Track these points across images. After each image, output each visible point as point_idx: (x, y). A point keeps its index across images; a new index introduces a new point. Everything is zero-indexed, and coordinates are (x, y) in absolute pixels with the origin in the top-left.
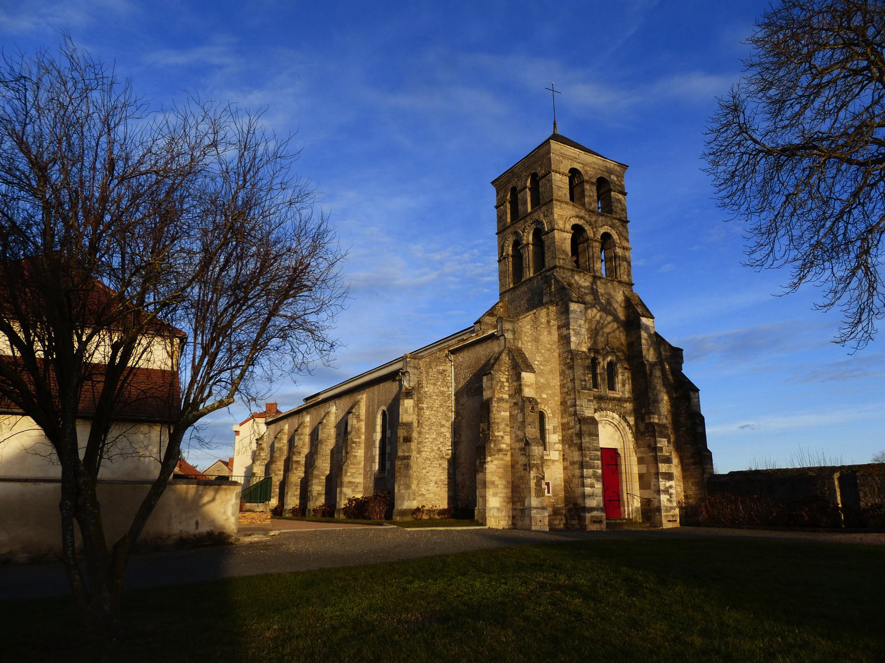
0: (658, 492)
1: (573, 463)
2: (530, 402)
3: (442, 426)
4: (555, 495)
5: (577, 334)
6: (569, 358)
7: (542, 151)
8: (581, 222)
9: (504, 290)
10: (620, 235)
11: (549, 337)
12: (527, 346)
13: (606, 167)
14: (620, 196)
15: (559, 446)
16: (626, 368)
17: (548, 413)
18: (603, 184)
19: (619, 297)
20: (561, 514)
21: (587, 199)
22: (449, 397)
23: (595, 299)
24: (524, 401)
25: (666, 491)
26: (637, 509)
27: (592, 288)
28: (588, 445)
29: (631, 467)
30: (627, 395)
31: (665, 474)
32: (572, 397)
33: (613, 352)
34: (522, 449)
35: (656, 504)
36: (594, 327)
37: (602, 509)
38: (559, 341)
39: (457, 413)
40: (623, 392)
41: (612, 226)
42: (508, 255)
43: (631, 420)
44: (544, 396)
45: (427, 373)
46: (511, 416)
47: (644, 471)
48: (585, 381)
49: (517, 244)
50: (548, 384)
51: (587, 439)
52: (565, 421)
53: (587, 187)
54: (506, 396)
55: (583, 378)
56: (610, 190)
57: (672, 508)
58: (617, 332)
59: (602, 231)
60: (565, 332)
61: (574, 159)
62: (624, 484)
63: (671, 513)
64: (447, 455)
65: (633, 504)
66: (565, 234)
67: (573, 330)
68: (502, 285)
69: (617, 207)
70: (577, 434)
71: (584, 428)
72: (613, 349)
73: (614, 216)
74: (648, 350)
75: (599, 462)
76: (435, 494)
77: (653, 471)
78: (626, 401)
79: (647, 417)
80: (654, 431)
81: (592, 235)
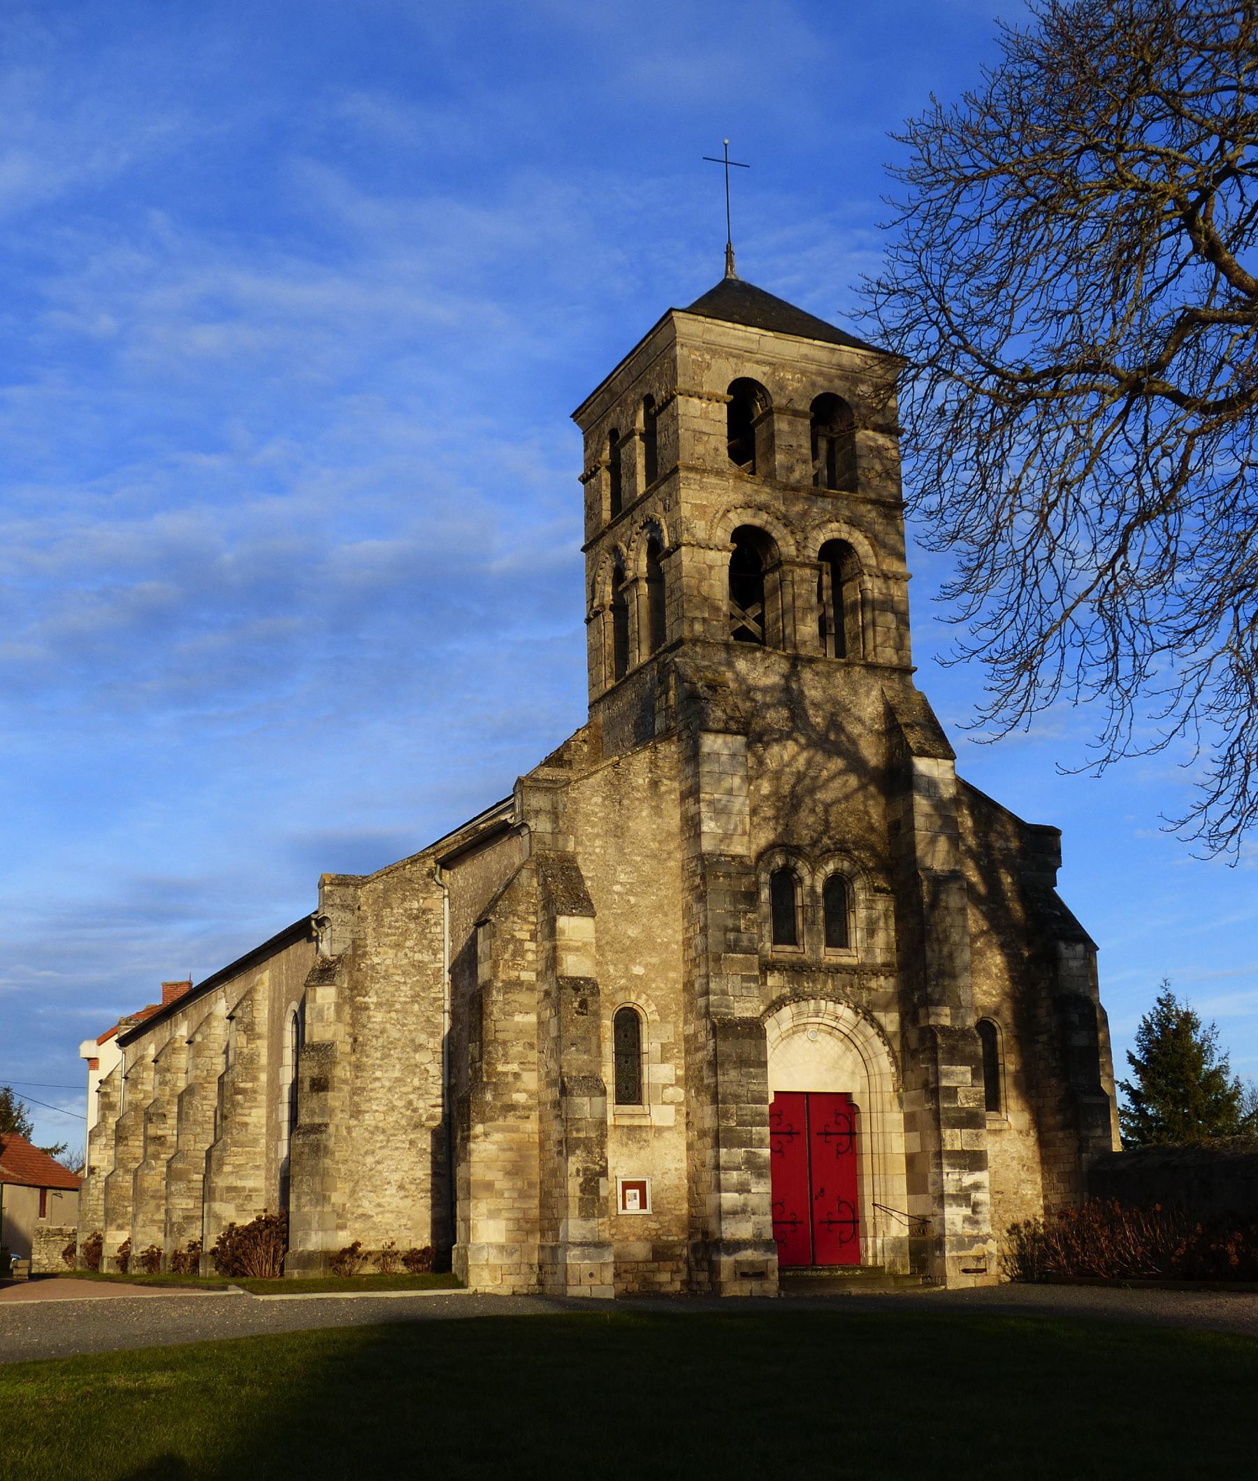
0: (941, 1199)
1: (702, 1134)
2: (577, 989)
3: (419, 1048)
4: (658, 1212)
5: (720, 811)
6: (705, 871)
7: (660, 340)
8: (759, 520)
9: (597, 696)
10: (876, 541)
11: (654, 823)
12: (591, 851)
13: (840, 367)
14: (882, 440)
15: (679, 1094)
16: (878, 890)
17: (649, 1012)
18: (829, 413)
19: (868, 705)
20: (672, 1258)
21: (780, 458)
22: (437, 974)
23: (793, 717)
24: (560, 988)
25: (963, 1197)
26: (897, 1245)
27: (787, 689)
28: (733, 1089)
29: (886, 1138)
30: (880, 959)
31: (962, 1154)
32: (703, 971)
33: (842, 849)
34: (557, 1104)
35: (937, 1230)
36: (786, 789)
37: (766, 1245)
38: (682, 831)
39: (455, 1016)
40: (869, 950)
41: (853, 523)
42: (602, 605)
43: (891, 1021)
44: (638, 970)
45: (379, 919)
46: (541, 1023)
47: (917, 1149)
48: (737, 929)
49: (619, 575)
50: (650, 939)
51: (733, 1074)
52: (690, 1030)
53: (781, 425)
54: (528, 976)
55: (730, 923)
56: (852, 428)
57: (975, 1239)
58: (860, 796)
59: (822, 537)
60: (693, 809)
61: (740, 355)
62: (867, 1181)
63: (973, 1252)
64: (431, 1118)
65: (886, 1230)
66: (712, 556)
67: (711, 803)
68: (593, 685)
69: (870, 468)
70: (710, 1063)
71: (726, 1047)
72: (843, 841)
73: (860, 494)
74: (933, 841)
75: (766, 1130)
76: (399, 1213)
77: (932, 1149)
78: (876, 973)
79: (922, 1012)
80: (935, 1048)
81: (792, 551)
